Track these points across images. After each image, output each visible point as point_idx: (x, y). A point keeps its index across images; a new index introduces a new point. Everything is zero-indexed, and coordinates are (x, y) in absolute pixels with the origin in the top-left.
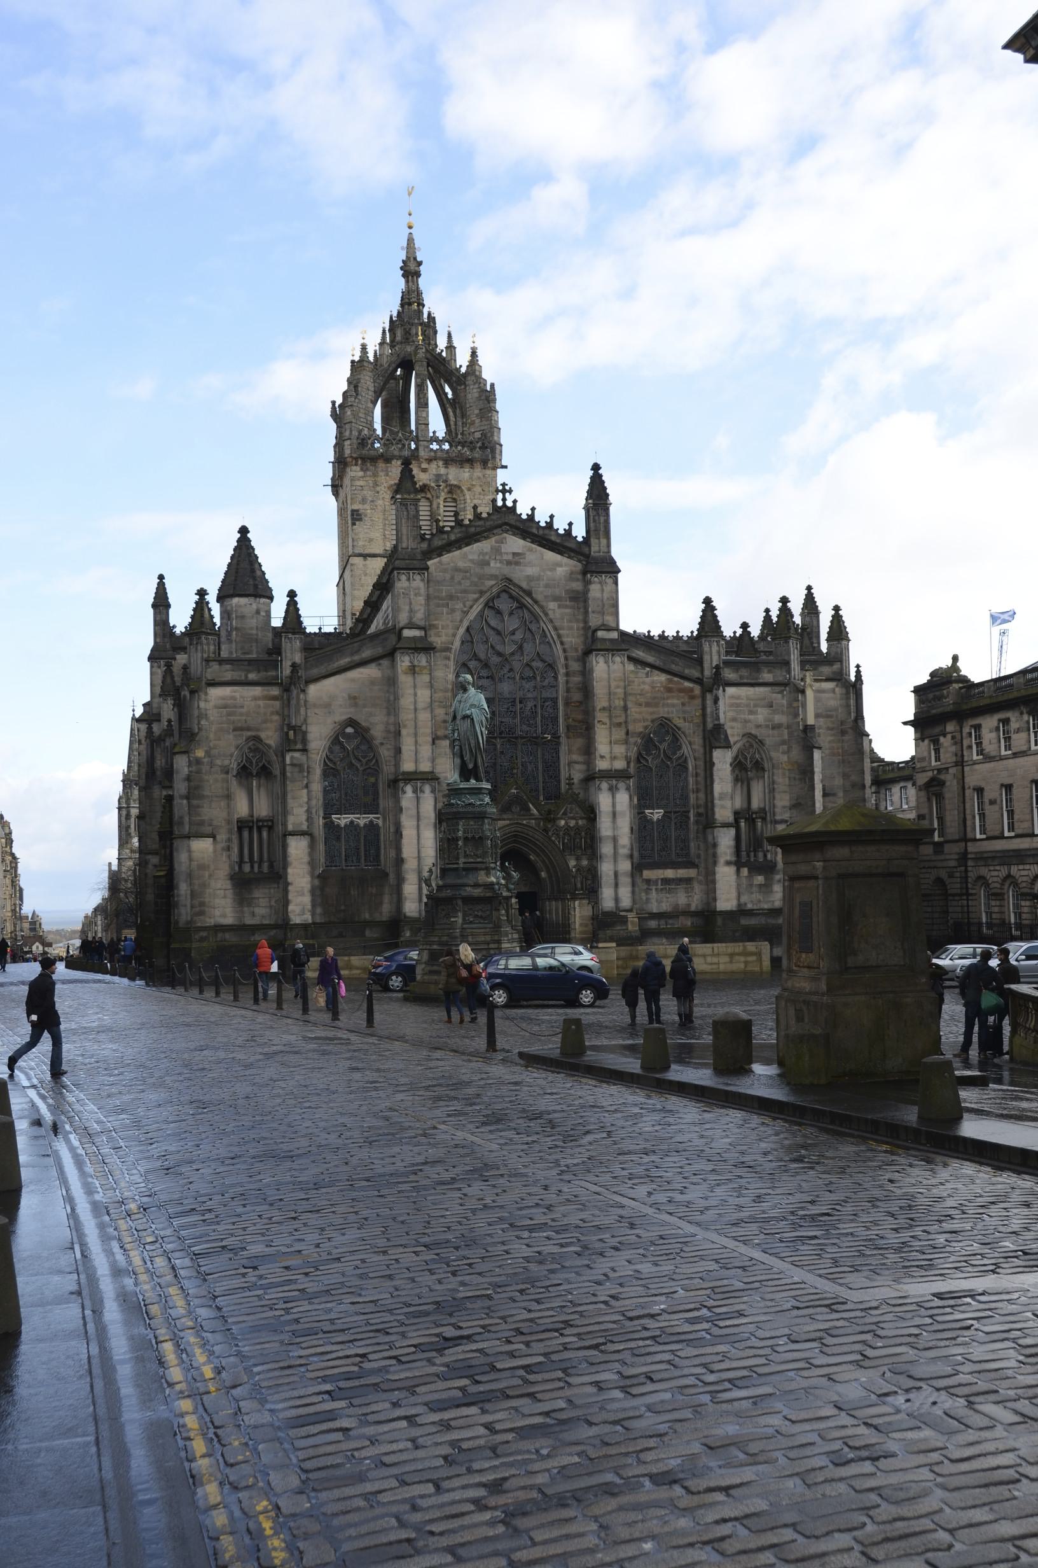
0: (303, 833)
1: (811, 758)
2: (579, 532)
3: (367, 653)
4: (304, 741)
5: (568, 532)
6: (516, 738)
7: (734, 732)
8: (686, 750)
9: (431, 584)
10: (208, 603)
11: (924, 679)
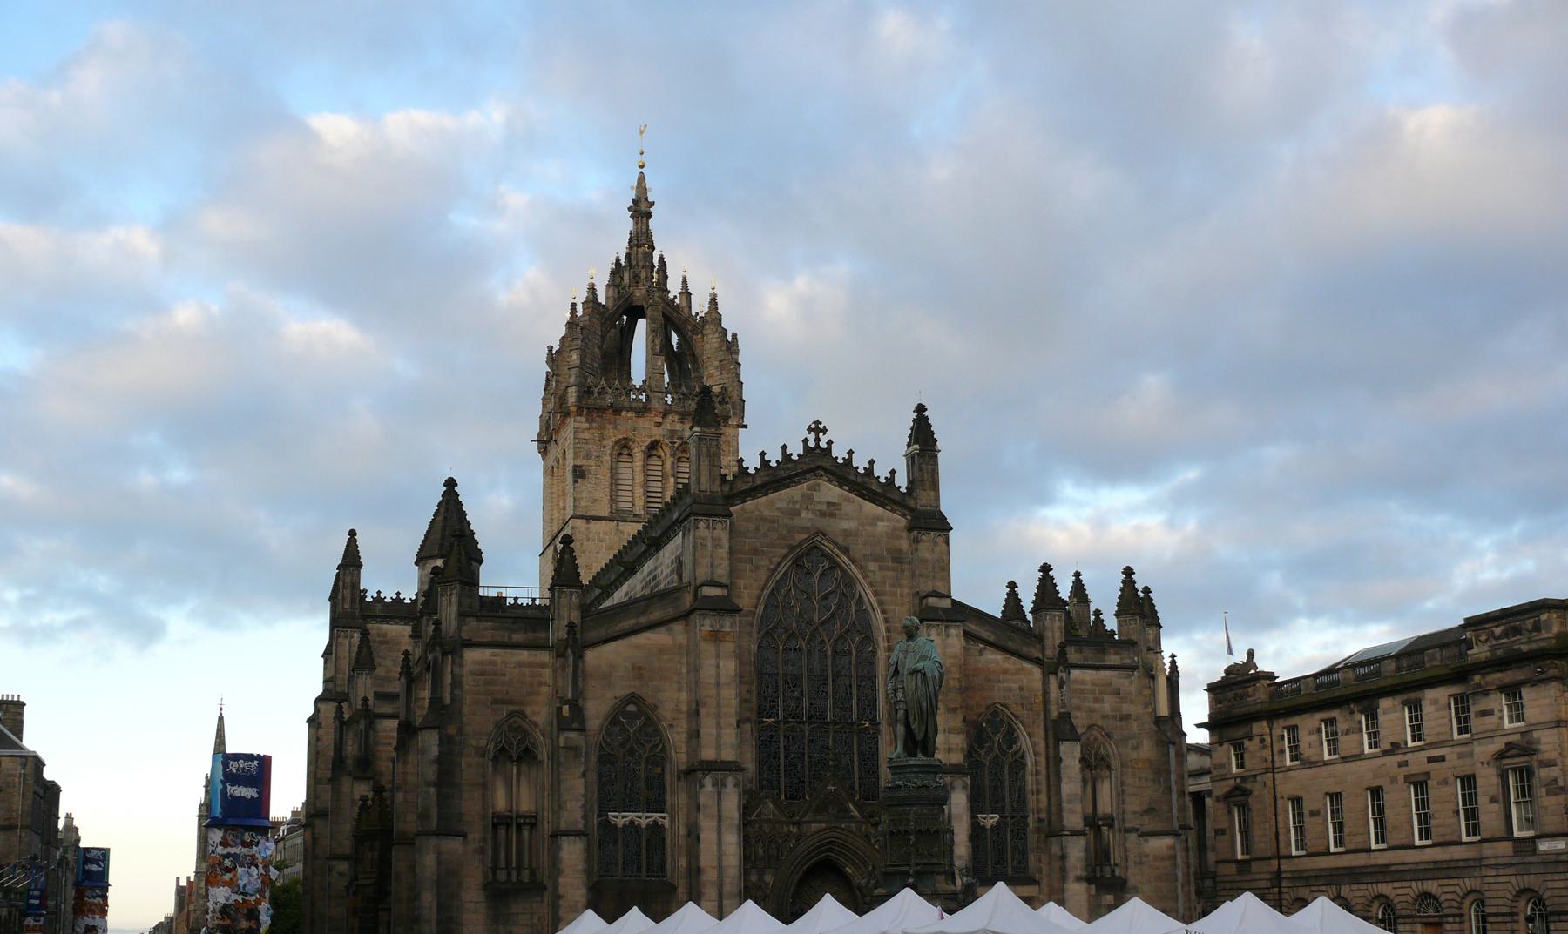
0: (577, 834)
1: (1168, 754)
2: (902, 481)
3: (656, 615)
4: (583, 721)
5: (890, 481)
6: (828, 724)
7: (1080, 721)
8: (1025, 743)
11: (1219, 675)
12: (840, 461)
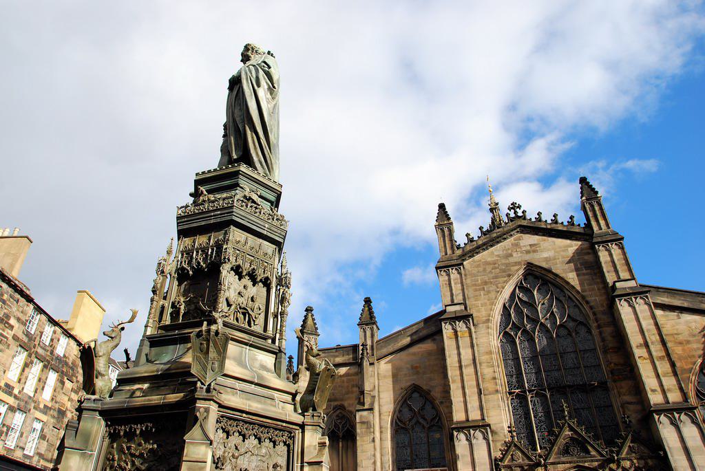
9: (468, 276)
10: (312, 315)
12: (533, 220)
